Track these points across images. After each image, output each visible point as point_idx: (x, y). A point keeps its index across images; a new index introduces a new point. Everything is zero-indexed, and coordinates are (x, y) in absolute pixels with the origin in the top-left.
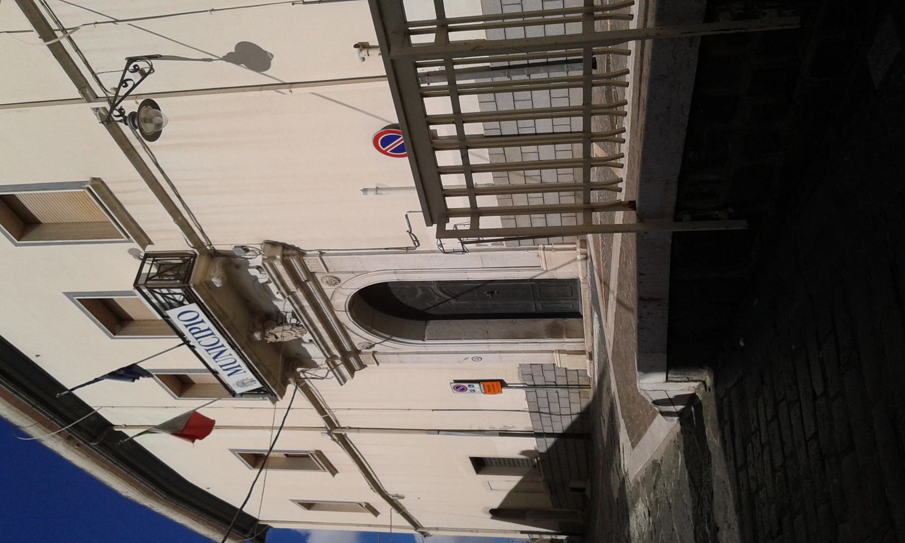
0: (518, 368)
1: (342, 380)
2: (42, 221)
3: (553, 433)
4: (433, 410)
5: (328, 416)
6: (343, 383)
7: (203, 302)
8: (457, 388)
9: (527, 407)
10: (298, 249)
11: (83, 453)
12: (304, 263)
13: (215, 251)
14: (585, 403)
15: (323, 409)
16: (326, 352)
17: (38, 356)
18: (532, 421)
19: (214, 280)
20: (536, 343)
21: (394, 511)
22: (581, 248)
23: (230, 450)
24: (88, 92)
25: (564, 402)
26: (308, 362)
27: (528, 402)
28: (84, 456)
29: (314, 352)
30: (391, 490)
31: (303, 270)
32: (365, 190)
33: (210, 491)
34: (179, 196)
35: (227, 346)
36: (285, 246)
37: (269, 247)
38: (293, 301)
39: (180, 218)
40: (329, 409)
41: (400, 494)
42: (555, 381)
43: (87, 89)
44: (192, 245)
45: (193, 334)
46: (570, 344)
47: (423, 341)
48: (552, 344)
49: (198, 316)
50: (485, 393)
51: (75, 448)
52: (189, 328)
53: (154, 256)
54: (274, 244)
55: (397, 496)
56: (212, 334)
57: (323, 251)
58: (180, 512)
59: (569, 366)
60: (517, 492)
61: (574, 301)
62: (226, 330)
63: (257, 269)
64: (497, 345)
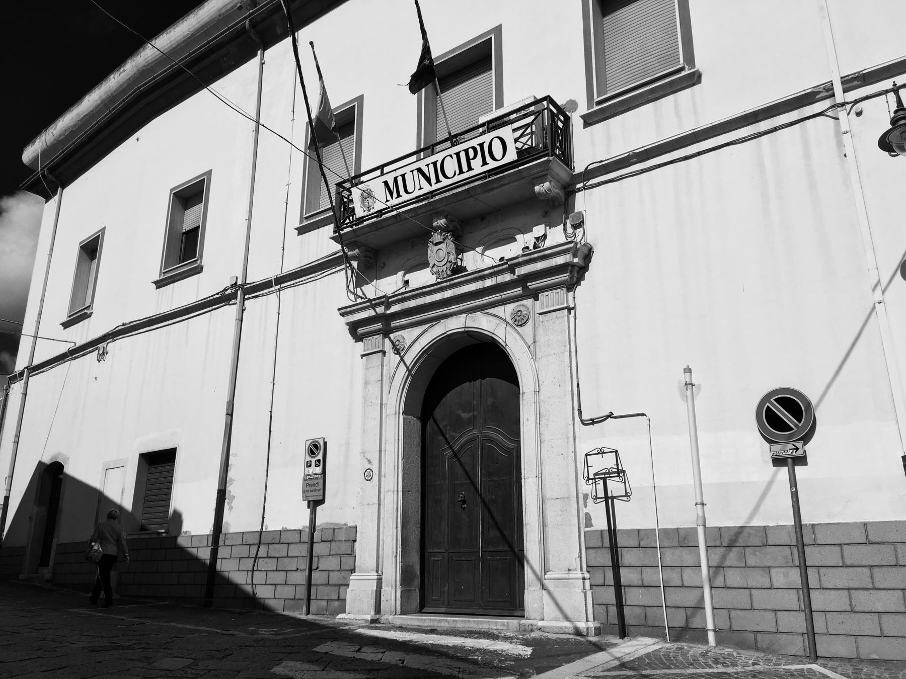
0: (346, 524)
1: (344, 312)
2: (604, 19)
3: (217, 559)
4: (271, 412)
5: (272, 286)
6: (343, 311)
7: (520, 168)
9: (269, 529)
10: (578, 283)
11: (227, 11)
12: (557, 289)
13: (575, 192)
14: (277, 606)
15: (281, 284)
16: (400, 297)
18: (243, 533)
19: (547, 185)
22: (595, 629)
23: (211, 170)
24: (856, 83)
25: (279, 577)
27: (281, 531)
28: (224, 10)
29: (389, 285)
30: (113, 347)
32: (688, 370)
35: (435, 187)
37: (586, 252)
39: (635, 160)
40: (280, 291)
41: (107, 357)
42: (320, 568)
43: (860, 82)
44: (590, 168)
45: (466, 151)
46: (392, 595)
48: (392, 572)
49: (493, 158)
50: (305, 480)
51: (238, 3)
52: (478, 148)
54: (588, 255)
55: (104, 353)
56: (461, 172)
57: (573, 312)
59: (352, 590)
60: (99, 501)
61: (446, 602)
62: (466, 187)
63: (544, 235)
64: (393, 502)
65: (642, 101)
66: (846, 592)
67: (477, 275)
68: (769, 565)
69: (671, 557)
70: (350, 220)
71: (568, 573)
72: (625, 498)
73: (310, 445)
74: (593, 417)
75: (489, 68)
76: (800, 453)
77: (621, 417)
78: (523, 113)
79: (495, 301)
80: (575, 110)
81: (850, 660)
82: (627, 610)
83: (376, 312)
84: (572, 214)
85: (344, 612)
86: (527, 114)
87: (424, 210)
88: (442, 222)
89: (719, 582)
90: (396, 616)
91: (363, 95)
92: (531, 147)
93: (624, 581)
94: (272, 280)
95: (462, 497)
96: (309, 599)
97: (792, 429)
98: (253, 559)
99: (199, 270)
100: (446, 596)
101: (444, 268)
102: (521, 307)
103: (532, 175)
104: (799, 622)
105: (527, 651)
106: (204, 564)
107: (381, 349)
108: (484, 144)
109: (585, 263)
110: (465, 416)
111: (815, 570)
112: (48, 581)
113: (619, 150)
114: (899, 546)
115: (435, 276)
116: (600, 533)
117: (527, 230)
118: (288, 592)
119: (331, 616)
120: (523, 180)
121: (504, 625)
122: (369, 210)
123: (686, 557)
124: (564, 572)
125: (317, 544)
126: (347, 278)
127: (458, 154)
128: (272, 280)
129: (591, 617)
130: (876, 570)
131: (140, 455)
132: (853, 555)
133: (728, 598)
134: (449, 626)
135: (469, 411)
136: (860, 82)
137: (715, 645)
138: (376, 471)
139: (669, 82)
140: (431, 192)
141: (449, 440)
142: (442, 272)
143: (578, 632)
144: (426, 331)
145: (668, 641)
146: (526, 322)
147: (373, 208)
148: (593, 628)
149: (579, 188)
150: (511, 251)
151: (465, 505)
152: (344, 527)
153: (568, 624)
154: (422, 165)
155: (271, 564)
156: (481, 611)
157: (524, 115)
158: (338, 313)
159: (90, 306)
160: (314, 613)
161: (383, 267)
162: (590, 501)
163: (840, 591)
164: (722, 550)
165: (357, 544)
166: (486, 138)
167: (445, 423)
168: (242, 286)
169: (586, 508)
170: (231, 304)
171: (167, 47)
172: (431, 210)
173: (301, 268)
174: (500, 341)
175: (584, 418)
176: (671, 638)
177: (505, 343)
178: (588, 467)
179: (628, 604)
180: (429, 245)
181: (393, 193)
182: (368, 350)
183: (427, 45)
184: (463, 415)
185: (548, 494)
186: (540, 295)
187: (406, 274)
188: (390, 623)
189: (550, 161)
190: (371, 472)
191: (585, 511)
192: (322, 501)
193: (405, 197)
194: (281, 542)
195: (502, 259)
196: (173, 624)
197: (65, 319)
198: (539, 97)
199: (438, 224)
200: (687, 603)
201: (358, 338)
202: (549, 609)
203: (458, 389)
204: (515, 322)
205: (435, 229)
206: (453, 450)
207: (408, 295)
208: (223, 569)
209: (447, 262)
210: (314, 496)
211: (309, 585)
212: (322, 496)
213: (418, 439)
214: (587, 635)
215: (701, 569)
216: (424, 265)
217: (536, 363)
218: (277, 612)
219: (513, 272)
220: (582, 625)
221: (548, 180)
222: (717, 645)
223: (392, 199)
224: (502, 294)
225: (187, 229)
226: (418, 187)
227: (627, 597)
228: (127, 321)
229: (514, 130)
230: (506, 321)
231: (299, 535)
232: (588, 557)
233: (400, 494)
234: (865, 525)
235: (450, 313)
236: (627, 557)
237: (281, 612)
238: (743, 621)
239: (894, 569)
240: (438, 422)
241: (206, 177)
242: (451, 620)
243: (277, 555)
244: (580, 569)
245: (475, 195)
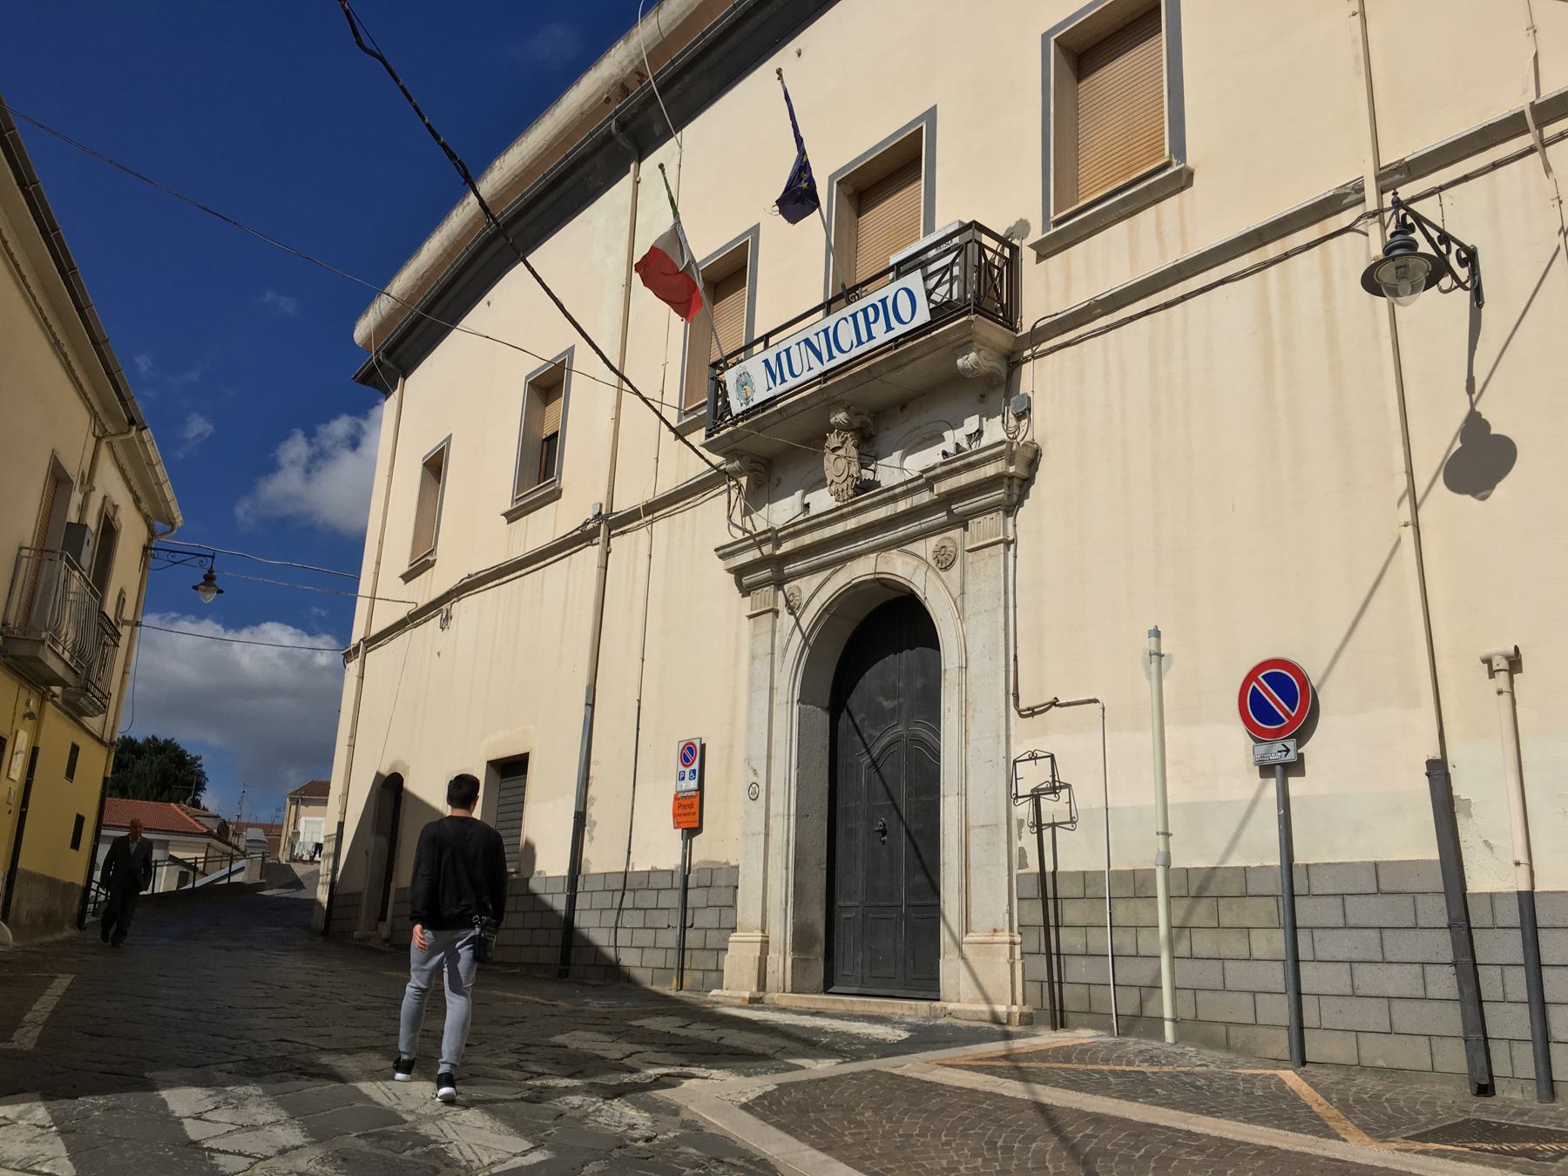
0: (727, 863)
1: (724, 553)
2: (1080, 86)
4: (639, 701)
5: (641, 518)
6: (721, 552)
7: (933, 333)
8: (691, 750)
9: (636, 869)
10: (1020, 503)
11: (591, 106)
14: (642, 976)
16: (791, 530)
17: (799, 54)
18: (605, 874)
19: (972, 356)
20: (787, 904)
21: (411, 608)
22: (1020, 1016)
25: (646, 937)
26: (756, 497)
27: (649, 872)
29: (782, 511)
30: (462, 609)
31: (976, 508)
32: (1157, 634)
33: (481, 306)
34: (1147, 313)
35: (828, 365)
36: (1027, 482)
37: (1030, 455)
41: (452, 623)
42: (695, 926)
43: (1403, 176)
44: (1038, 326)
45: (865, 311)
46: (780, 964)
47: (798, 701)
48: (781, 931)
50: (676, 798)
51: (603, 94)
52: (880, 305)
53: (1013, 263)
54: (1033, 462)
55: (448, 618)
56: (860, 343)
57: (1012, 546)
58: (445, 250)
59: (731, 956)
61: (860, 980)
62: (866, 365)
63: (978, 431)
64: (783, 831)
66: (1347, 966)
67: (886, 495)
68: (1248, 924)
69: (1123, 913)
71: (993, 935)
72: (1069, 826)
73: (684, 748)
74: (1031, 705)
76: (1292, 756)
77: (1069, 704)
78: (944, 247)
79: (914, 533)
80: (1027, 235)
81: (1348, 1067)
83: (762, 553)
85: (721, 987)
86: (949, 248)
87: (815, 400)
88: (841, 417)
89: (1183, 949)
92: (949, 301)
97: (1281, 720)
98: (616, 911)
99: (556, 495)
102: (946, 541)
103: (951, 343)
104: (1278, 1010)
106: (560, 917)
107: (771, 608)
108: (888, 300)
109: (1030, 471)
110: (887, 704)
111: (1307, 932)
112: (387, 940)
113: (1080, 297)
114: (1419, 897)
115: (834, 497)
117: (956, 424)
118: (656, 958)
121: (911, 1008)
124: (988, 934)
126: (729, 503)
130: (1387, 933)
131: (489, 762)
132: (1360, 911)
133: (1193, 973)
136: (1403, 176)
138: (763, 785)
139: (1147, 187)
141: (866, 741)
143: (995, 1019)
144: (827, 580)
145: (1116, 1035)
146: (951, 564)
147: (752, 400)
149: (1026, 358)
150: (930, 457)
151: (885, 838)
152: (725, 866)
153: (984, 1007)
157: (945, 251)
158: (714, 555)
159: (433, 550)
161: (777, 485)
163: (1340, 965)
164: (1187, 902)
165: (739, 890)
166: (889, 291)
170: (595, 545)
171: (518, 165)
172: (826, 399)
174: (919, 593)
176: (1120, 1032)
178: (1016, 779)
179: (1067, 981)
181: (775, 376)
183: (805, 160)
185: (971, 822)
186: (970, 522)
191: (1020, 844)
193: (792, 382)
196: (494, 992)
197: (405, 568)
201: (745, 591)
203: (879, 664)
206: (871, 756)
207: (801, 526)
211: (682, 949)
214: (1009, 1023)
216: (820, 483)
217: (964, 625)
218: (644, 986)
219: (932, 490)
220: (1001, 1009)
222: (1176, 1042)
224: (922, 521)
225: (548, 434)
226: (807, 367)
228: (474, 572)
233: (793, 820)
234: (1376, 865)
235: (857, 552)
236: (1070, 913)
238: (1216, 1008)
239: (1412, 932)
240: (853, 713)
241: (567, 356)
243: (645, 907)
245: (880, 376)
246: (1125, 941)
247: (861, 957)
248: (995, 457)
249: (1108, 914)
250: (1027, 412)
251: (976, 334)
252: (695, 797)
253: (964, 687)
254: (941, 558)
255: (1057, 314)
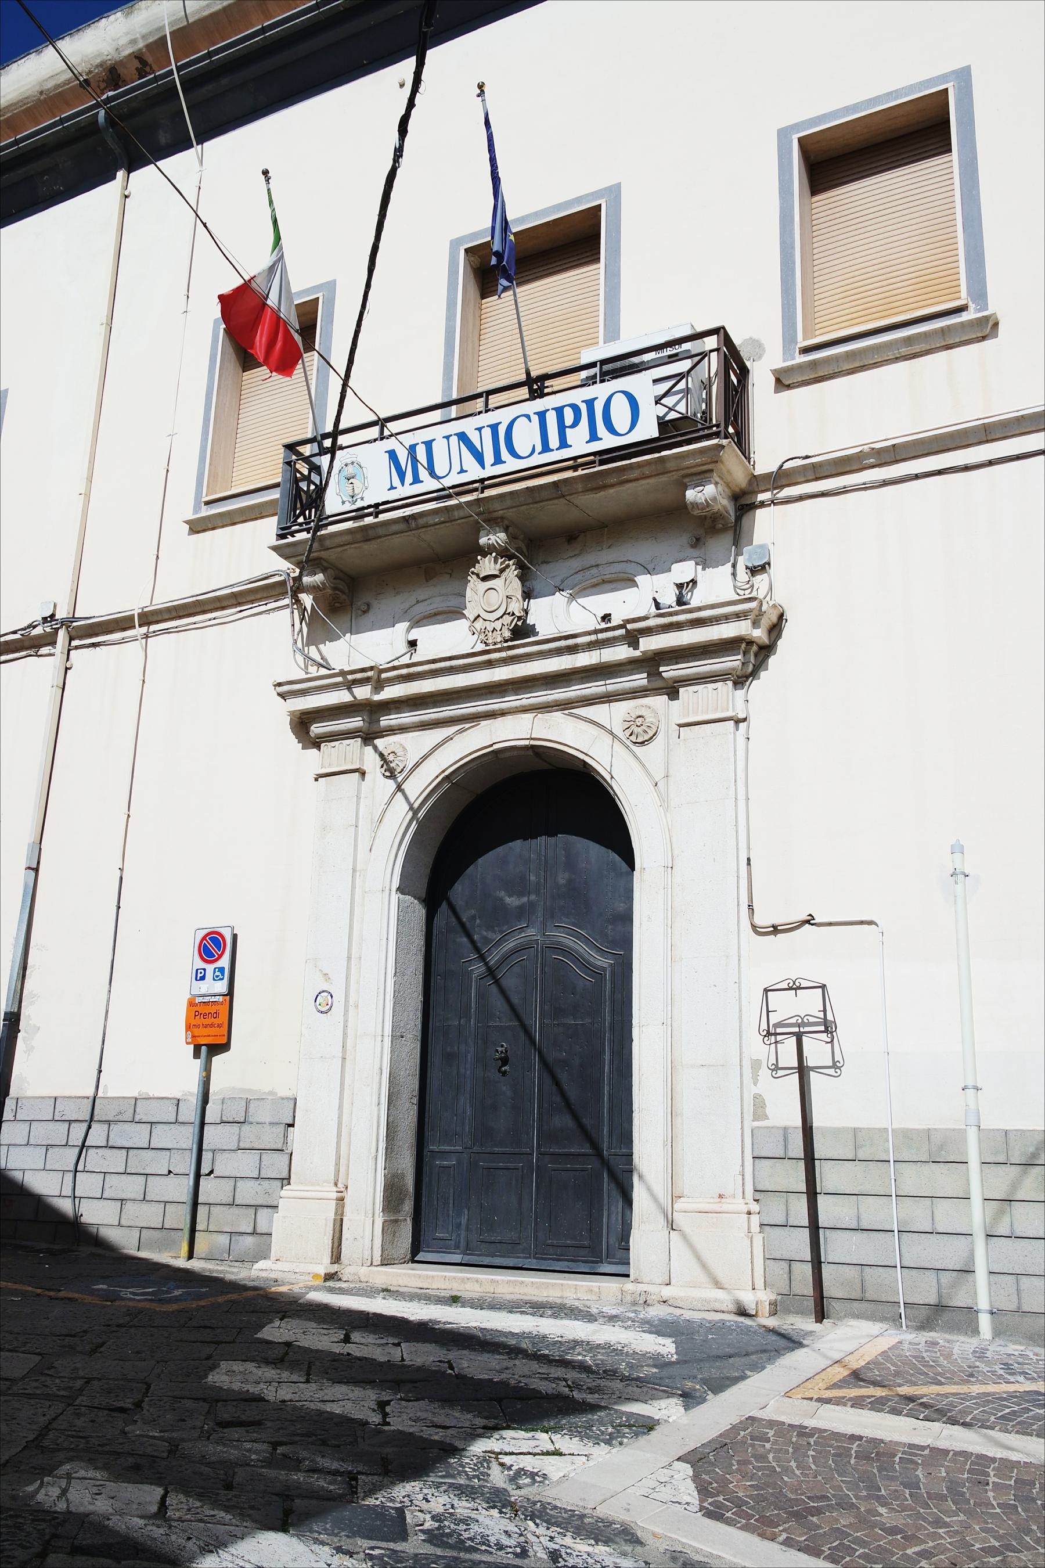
0: (271, 1093)
1: (286, 691)
9: (109, 1095)
10: (754, 674)
11: (57, 86)
13: (753, 507)
14: (126, 1242)
15: (149, 624)
16: (404, 671)
19: (709, 491)
25: (132, 1187)
27: (136, 1099)
28: (50, 84)
32: (958, 849)
35: (490, 471)
36: (766, 650)
37: (775, 619)
38: (601, 636)
39: (872, 460)
42: (216, 1173)
44: (787, 466)
45: (559, 411)
47: (398, 889)
50: (191, 1004)
52: (583, 407)
54: (776, 629)
56: (546, 448)
59: (284, 1217)
61: (463, 1244)
63: (692, 581)
65: (888, 356)
69: (913, 1179)
70: (305, 518)
72: (831, 1071)
73: (204, 938)
74: (776, 922)
75: (596, 257)
78: (669, 351)
80: (760, 358)
82: (826, 1270)
83: (355, 697)
84: (750, 547)
86: (676, 355)
88: (497, 538)
90: (373, 1268)
91: (335, 281)
92: (684, 418)
93: (823, 1221)
94: (134, 615)
95: (502, 1052)
96: (193, 1230)
98: (77, 1150)
100: (463, 1234)
101: (498, 625)
103: (683, 469)
105: (666, 1347)
107: (358, 767)
108: (596, 402)
116: (781, 1132)
118: (150, 1215)
119: (237, 1264)
120: (669, 475)
122: (354, 503)
123: (943, 1180)
124: (712, 1200)
125: (213, 1127)
127: (542, 415)
128: (134, 615)
129: (760, 1282)
134: (481, 1290)
135: (521, 894)
137: (991, 1338)
140: (482, 481)
141: (479, 945)
142: (493, 632)
147: (362, 499)
148: (768, 1303)
151: (506, 1068)
153: (720, 1294)
154: (468, 426)
155: (115, 1161)
156: (533, 1263)
157: (670, 356)
160: (203, 1256)
161: (364, 612)
162: (765, 1073)
166: (601, 391)
167: (473, 912)
168: (66, 623)
169: (755, 1084)
173: (194, 599)
175: (758, 921)
177: (610, 774)
178: (768, 1012)
180: (469, 578)
182: (330, 765)
184: (508, 900)
187: (412, 628)
188: (360, 1281)
189: (723, 447)
190: (329, 997)
191: (755, 1090)
192: (225, 1047)
193: (429, 484)
194: (137, 1119)
195: (606, 618)
198: (700, 329)
199: (490, 542)
200: (940, 1262)
202: (683, 1264)
203: (500, 850)
204: (631, 735)
205: (485, 552)
206: (486, 964)
208: (9, 1166)
209: (504, 614)
210: (209, 1036)
212: (226, 1037)
213: (418, 941)
215: (970, 1203)
216: (455, 613)
218: (126, 1251)
219: (634, 644)
220: (748, 1299)
221: (713, 481)
223: (403, 485)
224: (608, 682)
227: (829, 1249)
229: (655, 381)
230: (612, 734)
231: (176, 1107)
232: (756, 1173)
236: (828, 1177)
237: (133, 1252)
242: (486, 1279)
244: (741, 1194)
246: (919, 1216)
247: (466, 1216)
248: (738, 616)
249: (893, 1181)
250: (767, 566)
251: (722, 462)
252: (222, 1003)
253: (670, 890)
254: (636, 730)
255: (807, 457)
